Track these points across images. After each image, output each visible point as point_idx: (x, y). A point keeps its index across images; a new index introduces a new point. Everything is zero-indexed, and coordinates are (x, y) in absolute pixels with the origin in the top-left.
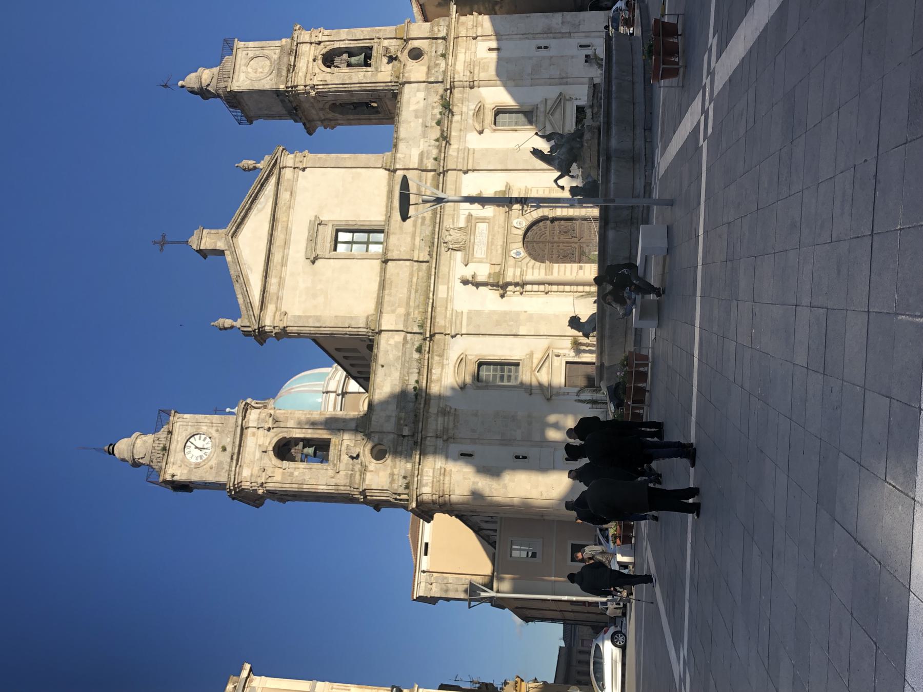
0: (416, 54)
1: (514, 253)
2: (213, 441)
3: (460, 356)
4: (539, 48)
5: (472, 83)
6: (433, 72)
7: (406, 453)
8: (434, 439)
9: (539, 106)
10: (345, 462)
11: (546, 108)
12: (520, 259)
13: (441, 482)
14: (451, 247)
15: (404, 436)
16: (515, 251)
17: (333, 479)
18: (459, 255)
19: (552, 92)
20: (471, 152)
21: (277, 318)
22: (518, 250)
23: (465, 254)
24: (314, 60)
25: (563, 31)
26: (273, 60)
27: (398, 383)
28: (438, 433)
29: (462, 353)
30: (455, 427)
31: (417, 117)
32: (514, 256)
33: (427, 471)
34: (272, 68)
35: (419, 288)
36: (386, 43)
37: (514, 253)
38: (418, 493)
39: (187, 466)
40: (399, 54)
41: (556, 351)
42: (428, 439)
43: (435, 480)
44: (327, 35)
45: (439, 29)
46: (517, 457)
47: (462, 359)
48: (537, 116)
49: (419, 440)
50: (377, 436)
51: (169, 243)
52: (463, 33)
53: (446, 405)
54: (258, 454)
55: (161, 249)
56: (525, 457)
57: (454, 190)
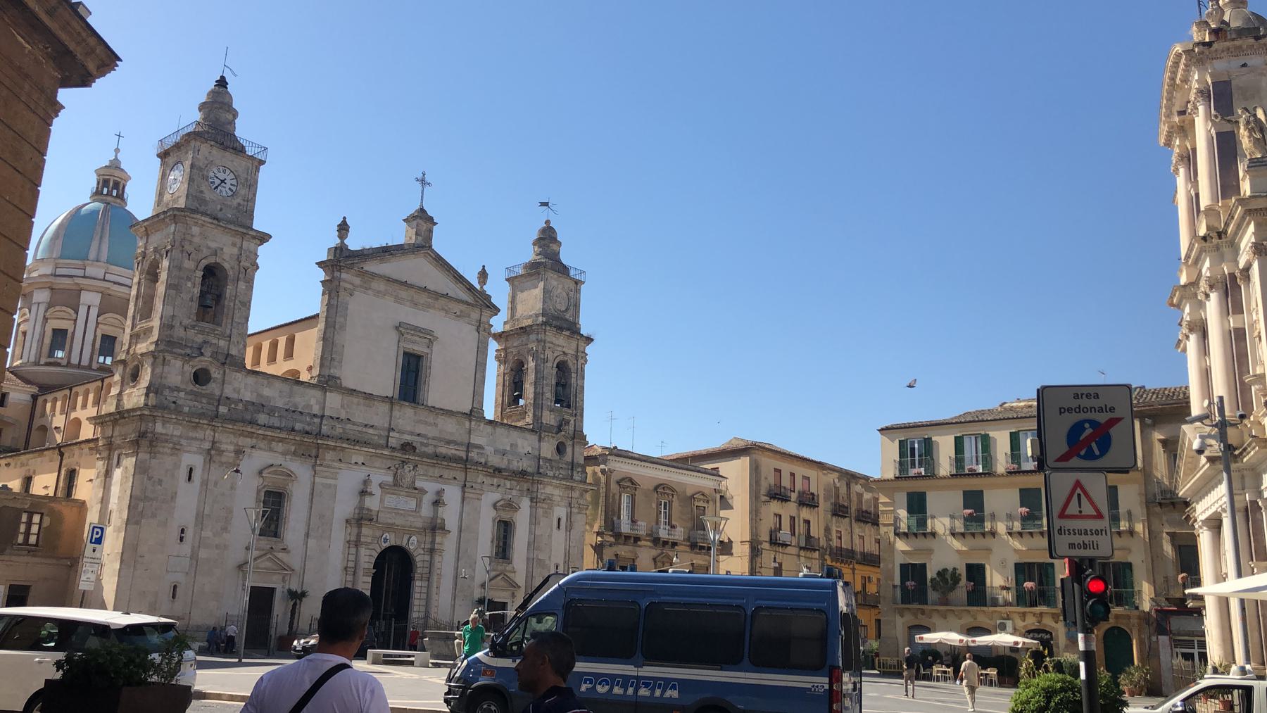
0: (560, 449)
2: (229, 199)
3: (294, 474)
4: (557, 567)
5: (535, 500)
7: (200, 407)
8: (211, 439)
10: (196, 339)
12: (379, 542)
13: (167, 444)
14: (399, 471)
15: (217, 407)
16: (388, 537)
17: (178, 324)
18: (389, 479)
20: (479, 496)
21: (348, 286)
23: (390, 485)
24: (564, 352)
28: (218, 445)
29: (297, 477)
30: (222, 464)
31: (512, 445)
32: (384, 536)
33: (178, 429)
35: (363, 435)
36: (572, 422)
38: (157, 418)
39: (206, 167)
40: (563, 433)
41: (287, 578)
42: (212, 433)
46: (183, 531)
49: (214, 424)
50: (219, 376)
51: (423, 187)
52: (576, 494)
54: (213, 245)
55: (417, 180)
56: (181, 539)
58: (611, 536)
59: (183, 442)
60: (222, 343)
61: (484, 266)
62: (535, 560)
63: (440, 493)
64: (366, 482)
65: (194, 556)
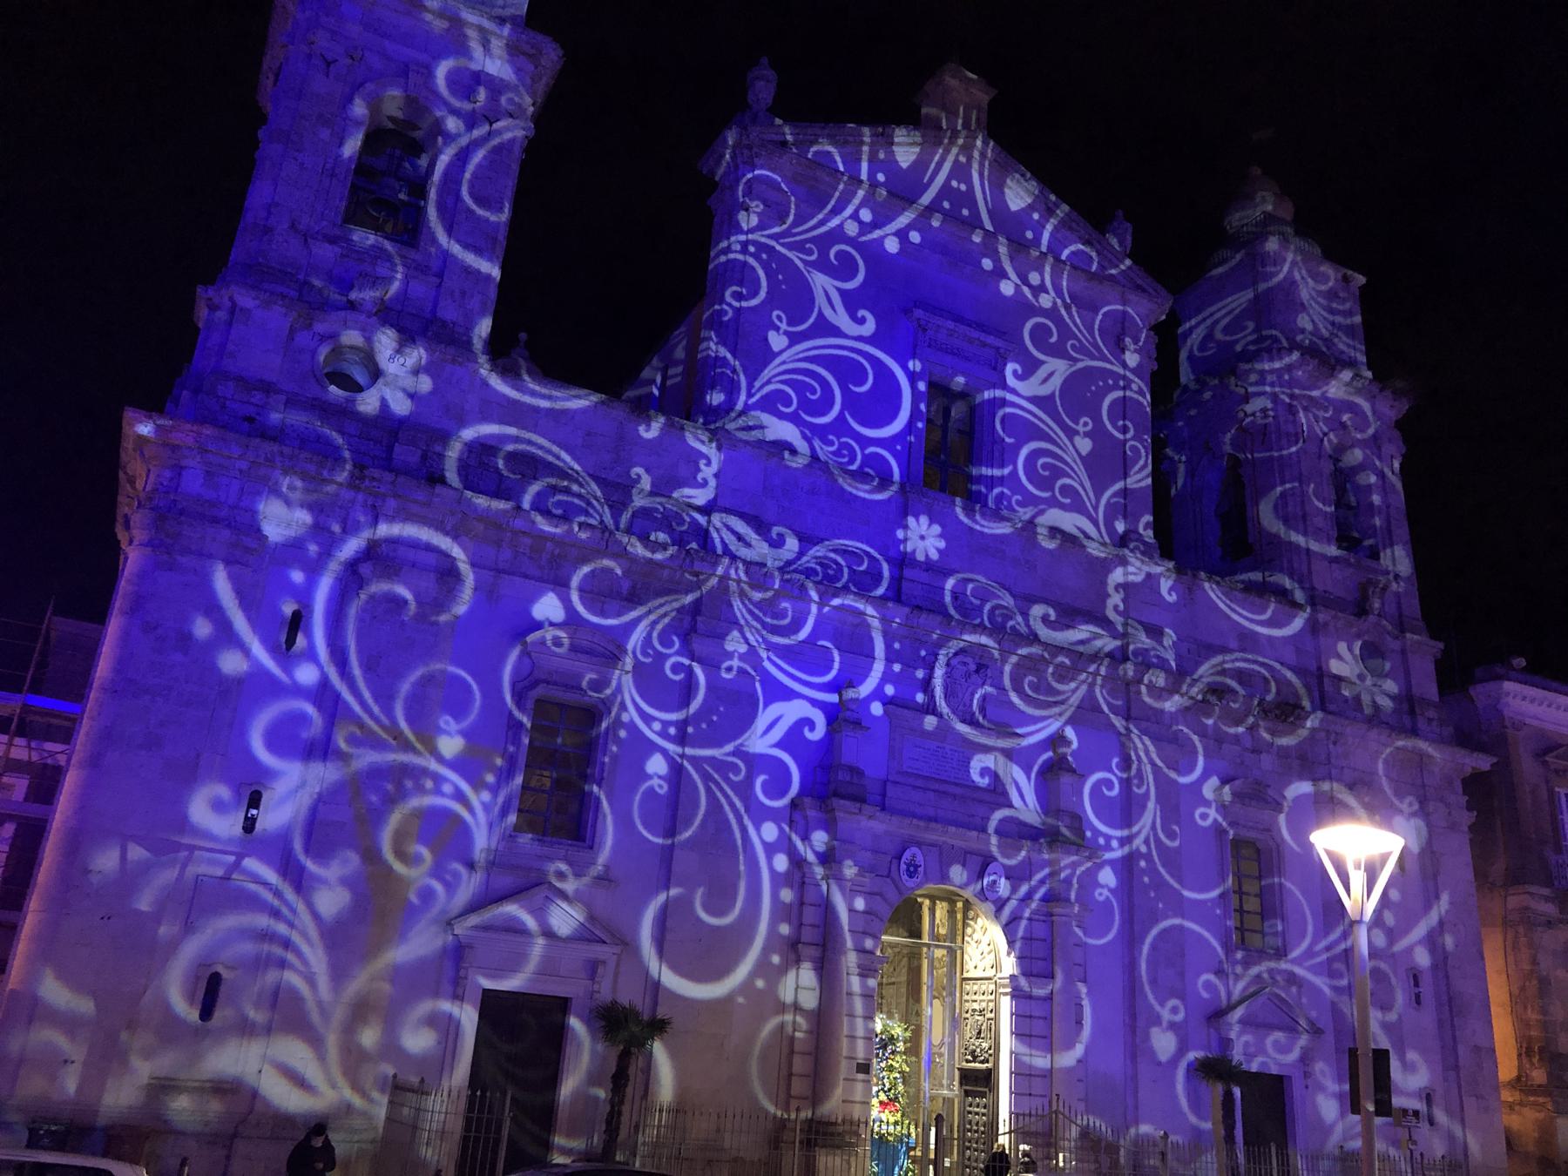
1: (914, 856)
16: (920, 859)
22: (921, 869)
25: (1461, 1050)
32: (907, 855)
37: (914, 856)
58: (1547, 899)
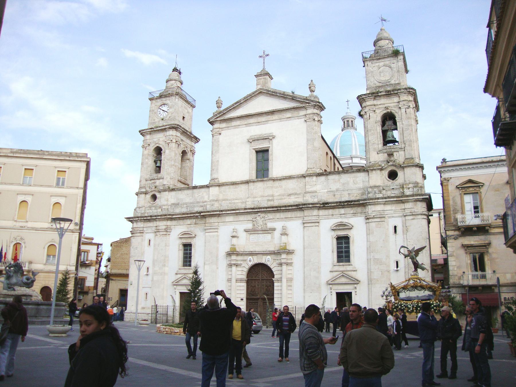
1: (250, 259)
6: (375, 190)
9: (351, 266)
11: (349, 271)
19: (361, 275)
20: (317, 224)
26: (389, 81)
27: (184, 202)
34: (383, 82)
37: (250, 259)
40: (391, 163)
43: (139, 228)
44: (406, 111)
45: (411, 188)
47: (192, 235)
48: (343, 265)
53: (172, 229)
57: (292, 217)
59: (145, 229)
60: (161, 180)
61: (312, 81)
62: (372, 260)
63: (284, 228)
64: (235, 230)
65: (152, 280)
